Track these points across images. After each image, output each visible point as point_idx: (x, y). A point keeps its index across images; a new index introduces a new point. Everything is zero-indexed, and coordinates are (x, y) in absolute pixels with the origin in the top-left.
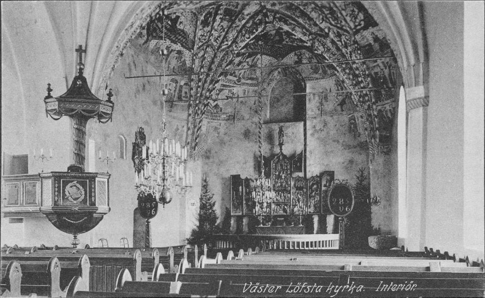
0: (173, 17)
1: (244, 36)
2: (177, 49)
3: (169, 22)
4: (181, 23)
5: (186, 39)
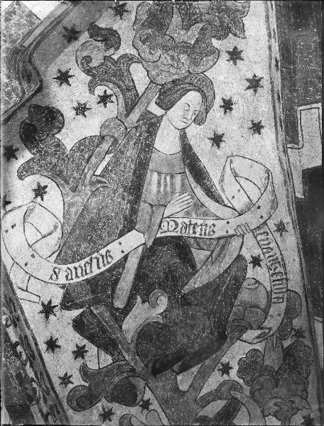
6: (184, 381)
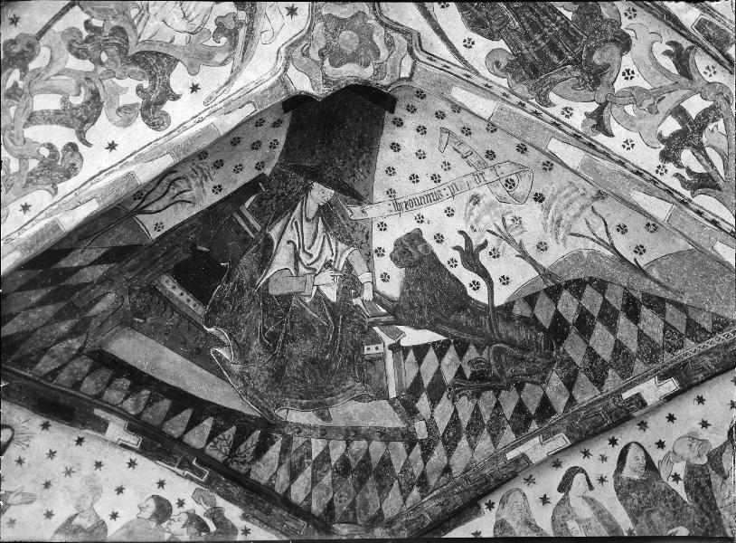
0: (393, 289)
4: (470, 257)
5: (658, 304)
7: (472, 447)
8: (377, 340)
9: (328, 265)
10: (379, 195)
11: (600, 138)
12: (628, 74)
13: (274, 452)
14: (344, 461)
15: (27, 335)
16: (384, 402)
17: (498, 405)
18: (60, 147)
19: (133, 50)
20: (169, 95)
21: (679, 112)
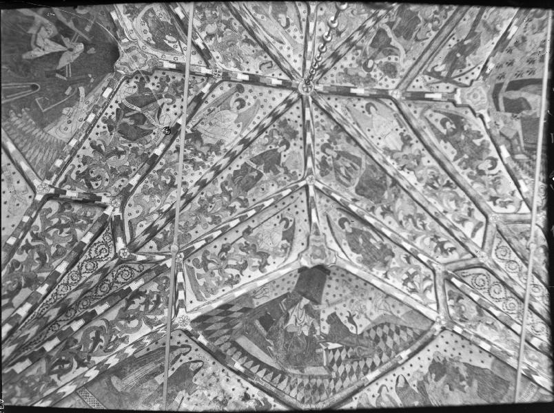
0: (326, 331)
1: (481, 173)
2: (425, 370)
3: (332, 346)
4: (350, 319)
5: (404, 328)
6: (121, 139)
7: (350, 380)
8: (320, 347)
9: (305, 324)
10: (323, 301)
11: (386, 280)
12: (394, 263)
13: (285, 382)
14: (308, 386)
15: (214, 331)
16: (322, 367)
17: (358, 366)
18: (234, 275)
19: (258, 251)
20: (266, 264)
21: (407, 273)
